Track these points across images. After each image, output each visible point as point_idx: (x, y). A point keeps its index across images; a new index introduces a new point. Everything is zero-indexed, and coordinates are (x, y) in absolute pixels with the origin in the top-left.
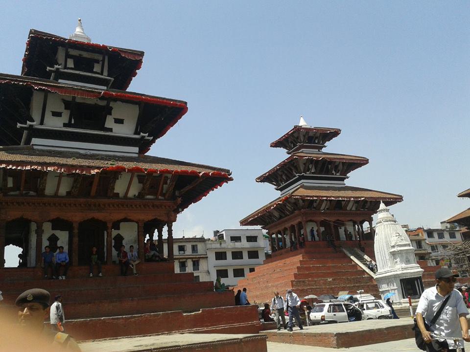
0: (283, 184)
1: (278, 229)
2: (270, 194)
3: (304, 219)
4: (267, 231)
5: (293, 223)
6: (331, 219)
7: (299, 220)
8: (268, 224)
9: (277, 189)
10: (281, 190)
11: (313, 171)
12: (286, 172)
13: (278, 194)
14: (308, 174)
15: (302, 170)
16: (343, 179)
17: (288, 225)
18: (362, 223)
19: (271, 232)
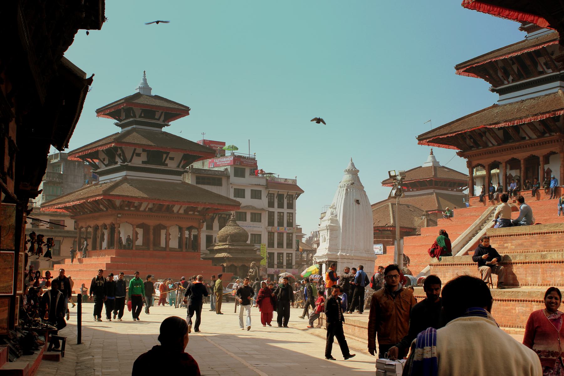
0: (509, 83)
4: (467, 160)
7: (553, 149)
8: (471, 147)
13: (495, 98)
17: (521, 155)
19: (475, 163)
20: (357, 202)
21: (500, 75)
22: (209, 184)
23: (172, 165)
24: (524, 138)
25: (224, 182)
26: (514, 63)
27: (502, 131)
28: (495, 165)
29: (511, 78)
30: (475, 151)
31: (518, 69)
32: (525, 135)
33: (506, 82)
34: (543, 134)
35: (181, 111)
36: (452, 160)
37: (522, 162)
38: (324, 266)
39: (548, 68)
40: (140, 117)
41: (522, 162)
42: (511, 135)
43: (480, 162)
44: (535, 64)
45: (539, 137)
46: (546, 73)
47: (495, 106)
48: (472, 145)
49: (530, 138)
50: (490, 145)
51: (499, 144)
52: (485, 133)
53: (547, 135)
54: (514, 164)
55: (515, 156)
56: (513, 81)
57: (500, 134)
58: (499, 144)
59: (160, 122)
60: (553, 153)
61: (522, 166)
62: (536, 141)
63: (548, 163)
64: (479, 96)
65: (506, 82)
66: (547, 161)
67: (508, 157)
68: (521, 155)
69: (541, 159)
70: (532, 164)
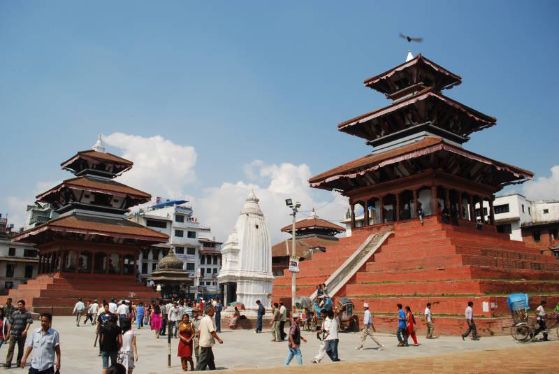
0: (381, 136)
2: (357, 150)
6: (460, 189)
7: (426, 184)
9: (368, 144)
10: (375, 145)
16: (461, 141)
17: (396, 191)
19: (355, 200)
20: (257, 227)
22: (156, 226)
23: (116, 206)
24: (398, 177)
25: (168, 225)
27: (378, 173)
28: (372, 203)
29: (383, 132)
30: (355, 190)
32: (399, 174)
35: (127, 165)
36: (335, 208)
37: (397, 196)
38: (225, 287)
39: (414, 122)
40: (93, 168)
41: (397, 196)
42: (387, 174)
45: (412, 174)
46: (413, 125)
47: (369, 156)
48: (353, 185)
49: (404, 176)
50: (368, 184)
51: (377, 183)
53: (420, 172)
54: (389, 199)
55: (390, 192)
56: (384, 135)
57: (377, 174)
58: (377, 183)
59: (110, 173)
60: (425, 188)
62: (410, 177)
64: (357, 150)
67: (384, 193)
68: (396, 191)
69: (414, 193)
70: (407, 197)
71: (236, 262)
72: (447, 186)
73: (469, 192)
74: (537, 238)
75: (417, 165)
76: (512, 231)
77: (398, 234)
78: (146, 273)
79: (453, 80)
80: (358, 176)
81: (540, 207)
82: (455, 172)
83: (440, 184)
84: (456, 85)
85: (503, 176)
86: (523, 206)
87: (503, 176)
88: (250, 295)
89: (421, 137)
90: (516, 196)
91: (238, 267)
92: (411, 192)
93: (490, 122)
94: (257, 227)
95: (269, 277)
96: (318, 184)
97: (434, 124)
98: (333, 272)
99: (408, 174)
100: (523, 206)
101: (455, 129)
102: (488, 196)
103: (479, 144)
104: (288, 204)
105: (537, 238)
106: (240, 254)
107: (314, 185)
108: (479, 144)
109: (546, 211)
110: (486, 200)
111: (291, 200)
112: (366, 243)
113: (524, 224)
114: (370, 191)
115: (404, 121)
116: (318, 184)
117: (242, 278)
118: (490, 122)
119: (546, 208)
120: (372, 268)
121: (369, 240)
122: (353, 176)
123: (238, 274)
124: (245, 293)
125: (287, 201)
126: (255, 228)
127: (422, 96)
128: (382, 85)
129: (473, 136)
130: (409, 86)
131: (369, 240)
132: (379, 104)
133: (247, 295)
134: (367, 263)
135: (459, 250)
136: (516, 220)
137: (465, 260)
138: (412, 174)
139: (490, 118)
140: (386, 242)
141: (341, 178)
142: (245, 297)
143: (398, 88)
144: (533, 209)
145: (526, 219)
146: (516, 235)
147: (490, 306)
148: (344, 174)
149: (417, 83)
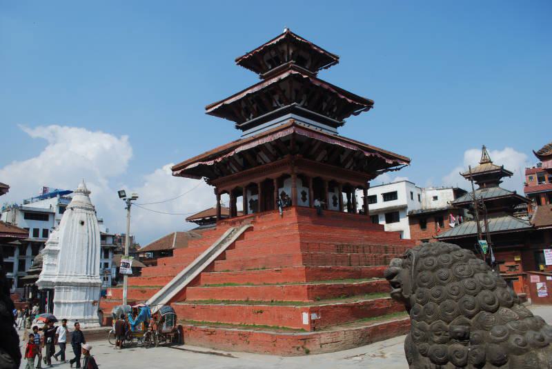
0: (250, 119)
1: (238, 185)
2: (226, 134)
3: (296, 171)
4: (215, 187)
5: (270, 176)
6: (328, 177)
8: (217, 176)
9: (238, 128)
10: (244, 128)
11: (306, 105)
12: (264, 99)
13: (239, 135)
14: (298, 106)
15: (294, 98)
16: (336, 125)
17: (258, 180)
18: (350, 190)
19: (221, 190)
20: (82, 223)
21: (243, 113)
24: (260, 164)
25: (50, 218)
26: (254, 103)
29: (252, 115)
31: (257, 108)
32: (261, 161)
33: (247, 119)
34: (276, 158)
41: (259, 185)
43: (224, 189)
44: (271, 100)
45: (272, 161)
46: (280, 107)
47: (238, 141)
48: (218, 174)
49: (265, 163)
50: (233, 172)
52: (228, 162)
53: (280, 158)
54: (253, 188)
56: (253, 118)
57: (240, 161)
61: (259, 189)
62: (270, 165)
63: (282, 186)
64: (226, 134)
65: (247, 119)
66: (281, 186)
67: (247, 182)
71: (55, 265)
72: (311, 174)
73: (338, 180)
74: (423, 226)
75: (279, 148)
76: (400, 219)
77: (257, 227)
78: (24, 270)
79: (328, 60)
80: (215, 162)
81: (430, 194)
82: (319, 158)
83: (301, 171)
84: (334, 64)
85: (376, 162)
86: (412, 193)
87: (376, 162)
88: (69, 304)
89: (286, 119)
90: (404, 183)
91: (56, 271)
92: (272, 180)
93: (367, 104)
94: (82, 223)
95: (93, 281)
96: (179, 172)
97: (303, 106)
98: (179, 272)
99: (268, 160)
100: (412, 193)
101: (329, 111)
102: (363, 185)
103: (354, 129)
104: (120, 197)
105: (423, 226)
106: (60, 255)
107: (175, 173)
108: (354, 129)
109: (435, 198)
110: (360, 188)
111: (124, 191)
112: (222, 238)
113: (412, 212)
114: (234, 179)
115: (272, 104)
116: (179, 172)
117: (59, 284)
118: (367, 104)
119: (435, 195)
120: (220, 265)
121: (226, 234)
122: (210, 163)
123: (54, 280)
124: (62, 301)
125: (119, 192)
126: (79, 225)
127: (292, 75)
128: (251, 62)
129: (350, 121)
130: (280, 64)
131: (226, 234)
132: (249, 81)
133: (65, 304)
134: (216, 262)
135: (304, 246)
136: (404, 208)
137: (305, 259)
138: (272, 161)
139: (362, 98)
140: (242, 237)
141: (199, 165)
142: (62, 306)
143: (270, 67)
144: (423, 196)
145: (415, 207)
146: (403, 225)
147: (310, 317)
148: (203, 161)
149: (289, 60)
